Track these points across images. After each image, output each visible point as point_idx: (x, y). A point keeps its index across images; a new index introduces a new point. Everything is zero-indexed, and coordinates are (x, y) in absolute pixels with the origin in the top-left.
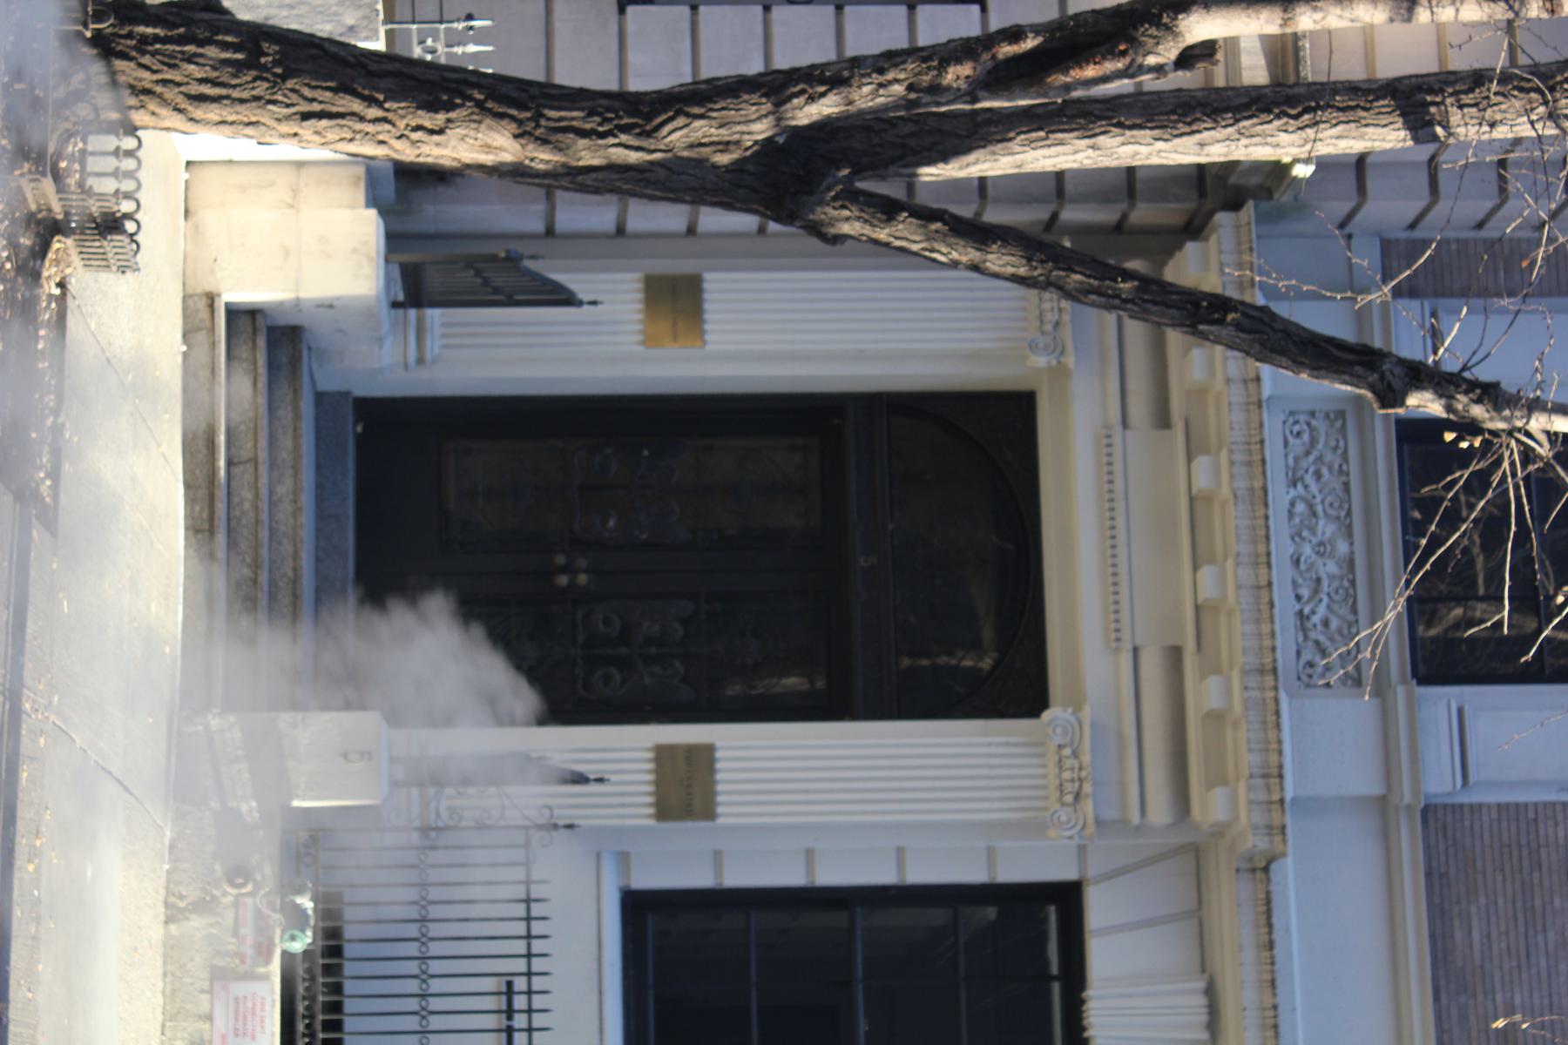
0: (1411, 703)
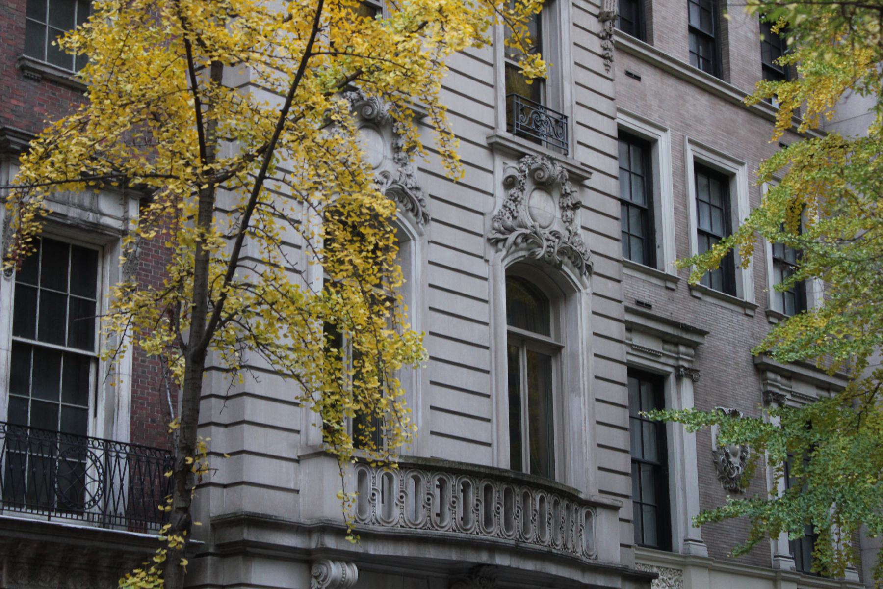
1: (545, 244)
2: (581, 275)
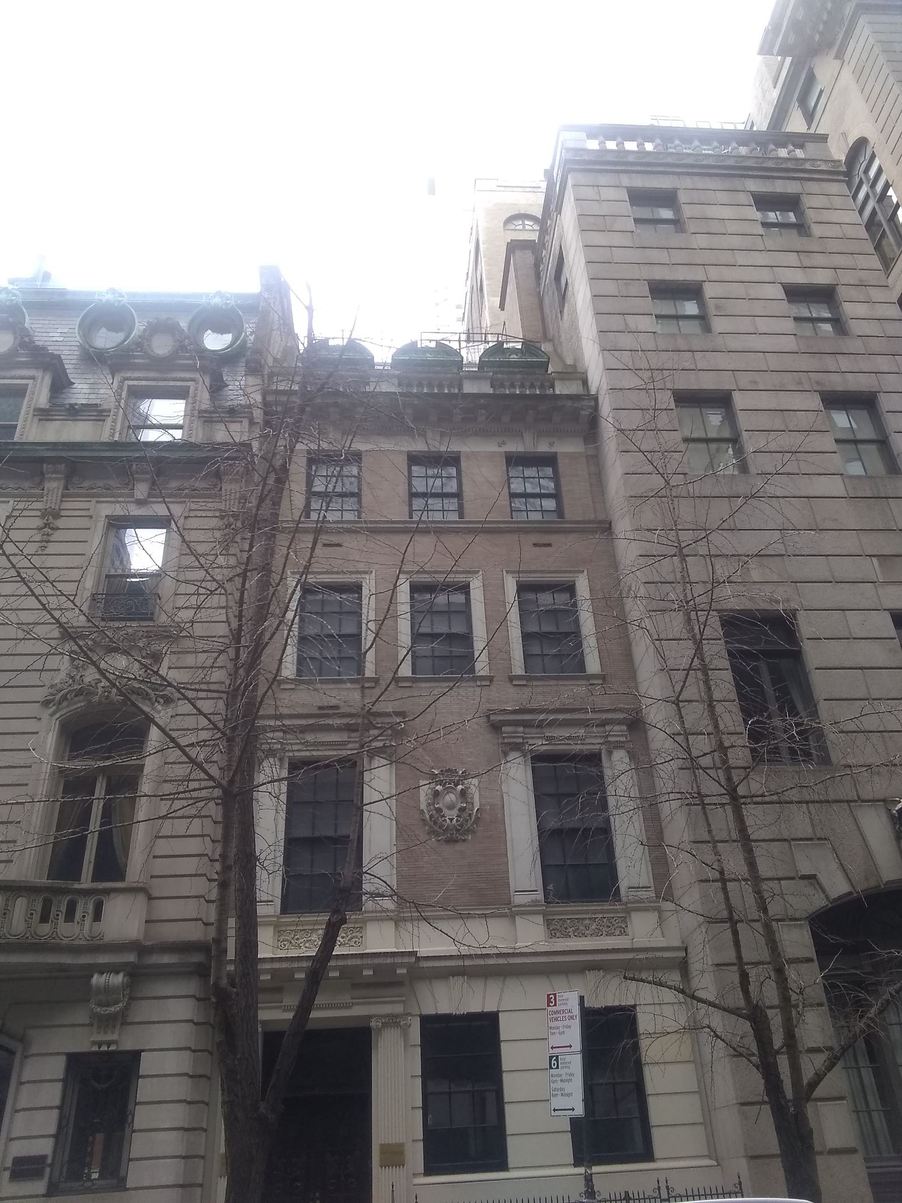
0: (366, 912)
1: (100, 691)
2: (153, 704)
